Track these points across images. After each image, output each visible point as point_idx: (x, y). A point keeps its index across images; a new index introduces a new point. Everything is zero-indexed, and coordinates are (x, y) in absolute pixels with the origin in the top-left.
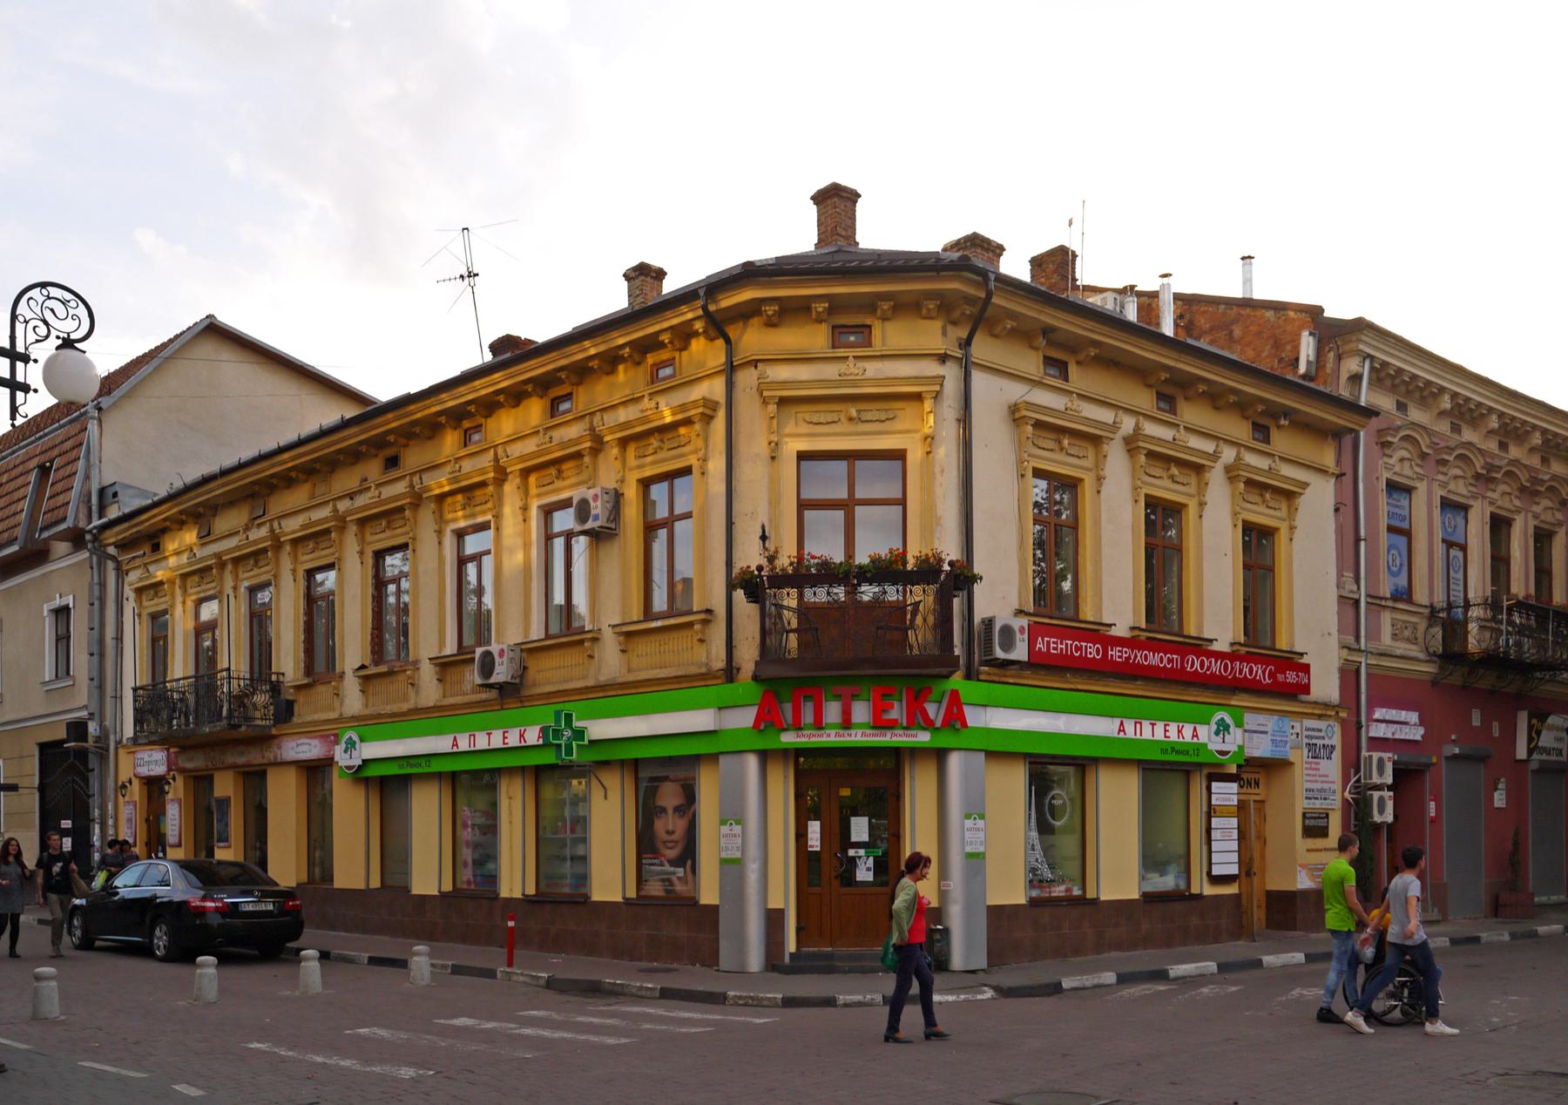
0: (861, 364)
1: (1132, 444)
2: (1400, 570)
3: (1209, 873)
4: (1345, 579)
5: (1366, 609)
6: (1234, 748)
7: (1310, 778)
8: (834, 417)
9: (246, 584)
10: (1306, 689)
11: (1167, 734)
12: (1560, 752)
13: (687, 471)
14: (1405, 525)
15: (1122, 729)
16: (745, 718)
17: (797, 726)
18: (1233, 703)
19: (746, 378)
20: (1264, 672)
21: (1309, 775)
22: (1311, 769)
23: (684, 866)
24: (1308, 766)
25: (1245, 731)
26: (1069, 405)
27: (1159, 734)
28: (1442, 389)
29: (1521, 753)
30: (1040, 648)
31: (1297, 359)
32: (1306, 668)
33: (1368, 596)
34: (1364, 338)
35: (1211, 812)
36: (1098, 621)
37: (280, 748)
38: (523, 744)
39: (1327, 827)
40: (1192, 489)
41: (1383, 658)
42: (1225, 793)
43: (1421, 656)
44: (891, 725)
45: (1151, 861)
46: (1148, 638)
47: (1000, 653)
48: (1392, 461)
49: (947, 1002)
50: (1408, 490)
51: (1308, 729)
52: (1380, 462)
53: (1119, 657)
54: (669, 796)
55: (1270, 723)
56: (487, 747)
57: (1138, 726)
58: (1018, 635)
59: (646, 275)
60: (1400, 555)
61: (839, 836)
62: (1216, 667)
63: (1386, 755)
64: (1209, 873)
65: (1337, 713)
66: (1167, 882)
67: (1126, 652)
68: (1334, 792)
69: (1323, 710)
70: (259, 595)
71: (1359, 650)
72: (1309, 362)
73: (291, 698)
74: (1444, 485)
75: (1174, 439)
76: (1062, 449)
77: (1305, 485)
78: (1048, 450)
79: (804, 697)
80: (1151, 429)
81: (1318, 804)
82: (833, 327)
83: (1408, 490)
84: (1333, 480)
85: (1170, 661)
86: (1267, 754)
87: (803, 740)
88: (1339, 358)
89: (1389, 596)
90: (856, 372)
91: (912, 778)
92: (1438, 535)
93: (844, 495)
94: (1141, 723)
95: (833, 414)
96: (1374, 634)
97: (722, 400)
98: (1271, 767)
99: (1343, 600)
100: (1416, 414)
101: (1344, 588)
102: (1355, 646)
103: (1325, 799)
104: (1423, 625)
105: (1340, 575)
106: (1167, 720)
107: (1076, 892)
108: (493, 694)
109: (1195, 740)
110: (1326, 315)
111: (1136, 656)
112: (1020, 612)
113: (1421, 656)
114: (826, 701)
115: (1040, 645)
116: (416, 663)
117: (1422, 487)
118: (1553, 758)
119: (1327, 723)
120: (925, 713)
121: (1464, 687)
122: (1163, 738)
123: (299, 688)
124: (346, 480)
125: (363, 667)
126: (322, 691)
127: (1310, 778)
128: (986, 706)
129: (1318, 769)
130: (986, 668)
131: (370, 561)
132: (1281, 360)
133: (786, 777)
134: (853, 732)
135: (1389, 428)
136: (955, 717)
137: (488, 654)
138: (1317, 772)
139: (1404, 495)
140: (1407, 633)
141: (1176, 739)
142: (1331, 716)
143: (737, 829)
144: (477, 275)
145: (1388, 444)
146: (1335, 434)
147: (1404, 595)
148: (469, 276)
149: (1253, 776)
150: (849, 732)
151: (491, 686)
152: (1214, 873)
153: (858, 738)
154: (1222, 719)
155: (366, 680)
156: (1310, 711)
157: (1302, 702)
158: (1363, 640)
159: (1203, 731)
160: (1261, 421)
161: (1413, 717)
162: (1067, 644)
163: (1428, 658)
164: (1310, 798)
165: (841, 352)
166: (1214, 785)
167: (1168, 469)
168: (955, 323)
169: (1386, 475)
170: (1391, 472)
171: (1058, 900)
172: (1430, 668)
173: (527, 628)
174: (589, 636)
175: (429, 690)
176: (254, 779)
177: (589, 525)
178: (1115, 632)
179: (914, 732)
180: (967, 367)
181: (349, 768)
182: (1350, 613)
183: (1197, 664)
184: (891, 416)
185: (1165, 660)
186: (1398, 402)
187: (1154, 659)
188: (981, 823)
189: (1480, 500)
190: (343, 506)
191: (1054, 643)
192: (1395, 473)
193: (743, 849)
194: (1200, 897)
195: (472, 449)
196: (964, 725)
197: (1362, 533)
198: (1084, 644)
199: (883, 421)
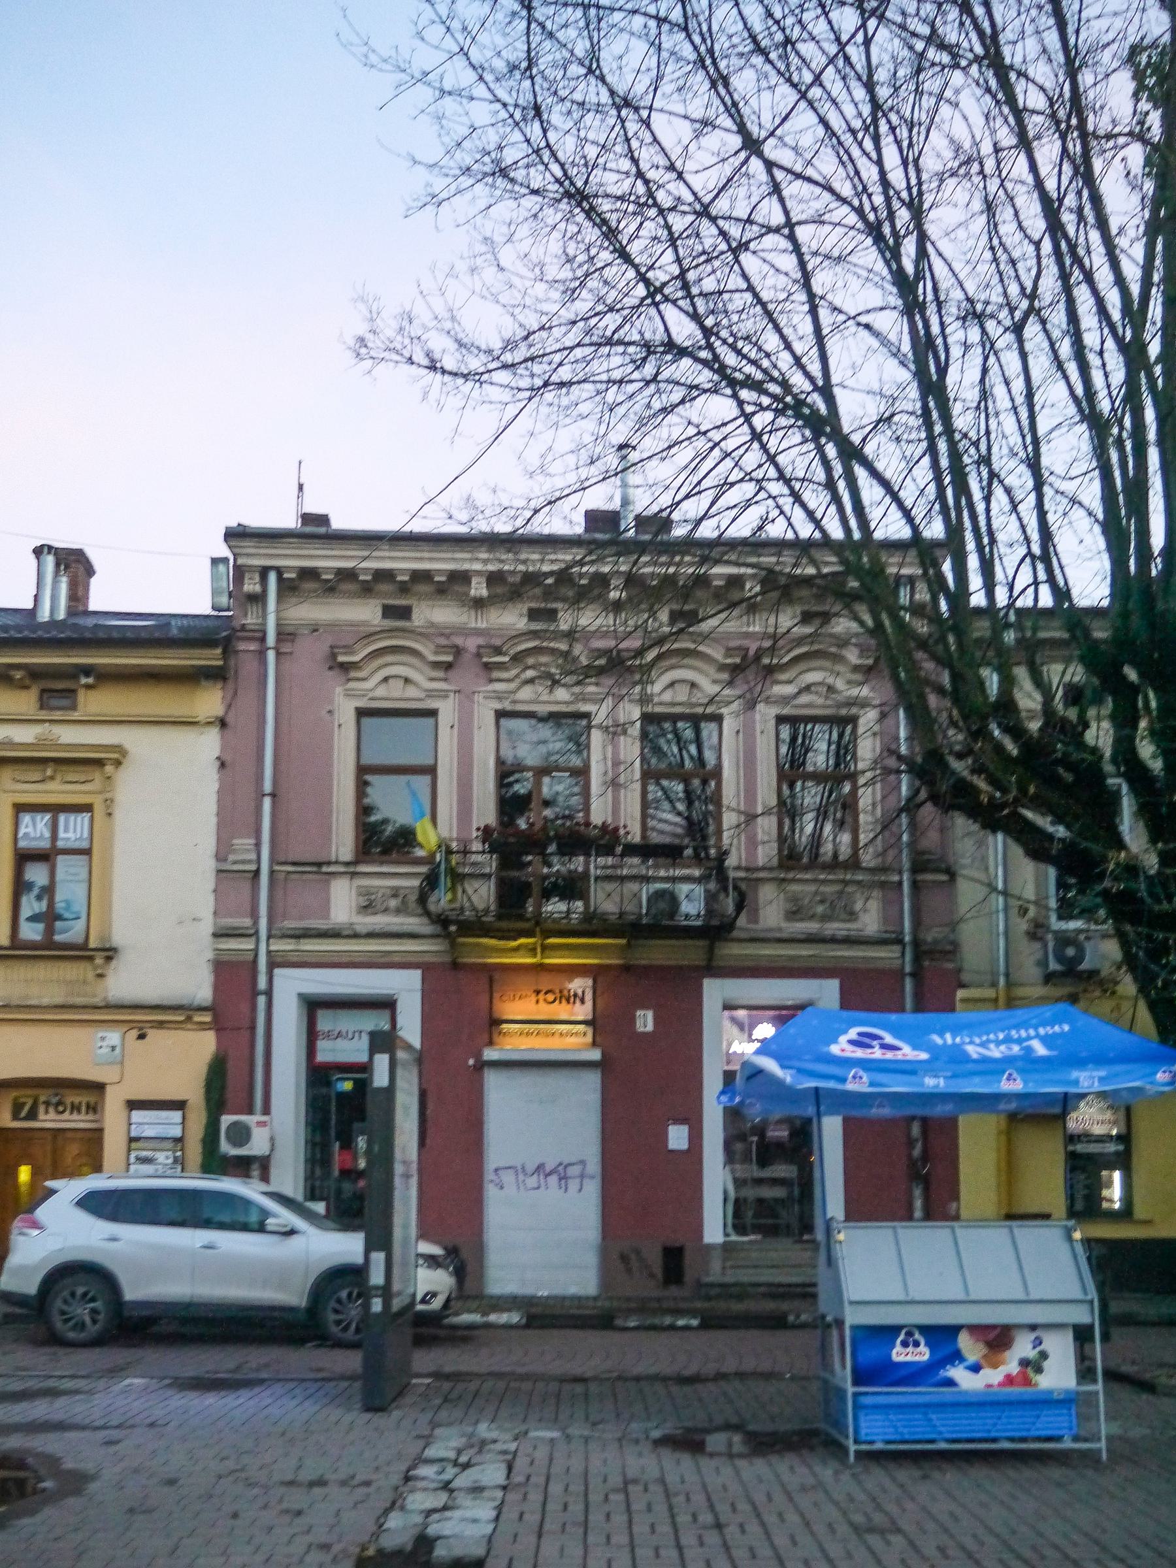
50: (433, 713)
96: (325, 908)
117: (447, 710)
146: (217, 675)
192: (372, 699)
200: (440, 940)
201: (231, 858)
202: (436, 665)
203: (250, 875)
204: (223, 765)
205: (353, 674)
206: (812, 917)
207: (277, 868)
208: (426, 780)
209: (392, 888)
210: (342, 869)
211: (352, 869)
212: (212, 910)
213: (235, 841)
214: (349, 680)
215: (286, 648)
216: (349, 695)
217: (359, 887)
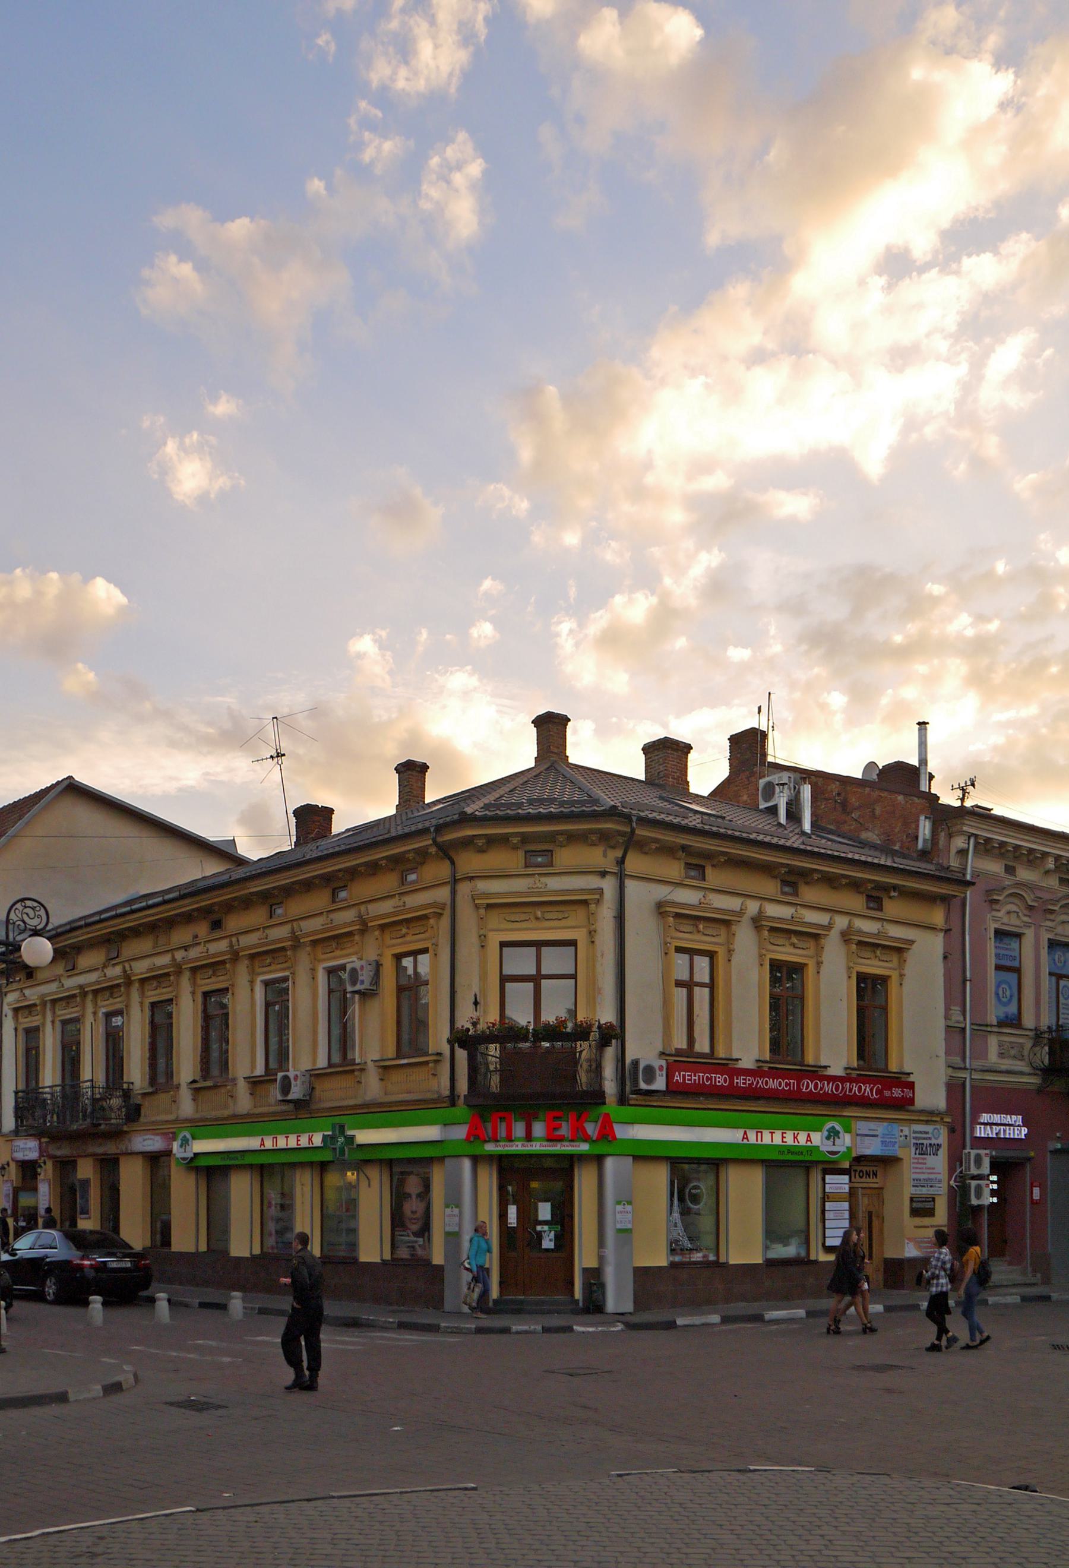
0: (544, 880)
1: (758, 922)
2: (1010, 1000)
3: (824, 1244)
4: (952, 1012)
5: (971, 1035)
6: (843, 1149)
7: (918, 1171)
8: (524, 917)
9: (104, 1010)
10: (911, 1101)
11: (784, 1140)
13: (425, 951)
14: (1016, 964)
15: (745, 1137)
16: (460, 1132)
17: (495, 1139)
18: (845, 1114)
19: (464, 888)
20: (871, 1090)
21: (917, 1168)
22: (918, 1163)
23: (423, 1237)
24: (916, 1161)
25: (857, 1135)
26: (703, 900)
27: (777, 1139)
28: (1045, 855)
30: (677, 1080)
31: (917, 838)
32: (911, 1086)
33: (972, 1024)
34: (966, 822)
35: (825, 1198)
36: (728, 1057)
37: (130, 1141)
38: (311, 1145)
39: (933, 1209)
40: (811, 952)
41: (988, 1073)
42: (838, 1183)
43: (1027, 1069)
44: (560, 1139)
45: (773, 1234)
46: (770, 1068)
47: (643, 1086)
48: (999, 914)
49: (589, 1332)
50: (1019, 936)
51: (915, 1132)
52: (989, 915)
53: (743, 1084)
54: (413, 1185)
55: (880, 1128)
56: (286, 1147)
57: (759, 1134)
58: (658, 1072)
59: (413, 770)
60: (1010, 988)
61: (527, 1216)
62: (829, 1088)
63: (982, 1152)
64: (824, 1244)
65: (942, 1119)
66: (790, 1250)
67: (749, 1080)
68: (940, 1181)
69: (930, 1116)
70: (113, 1019)
71: (965, 1069)
72: (925, 840)
73: (139, 1102)
74: (1050, 930)
75: (792, 917)
76: (699, 932)
77: (911, 942)
78: (687, 933)
79: (501, 1118)
80: (773, 910)
81: (924, 1191)
82: (526, 852)
83: (1019, 936)
84: (942, 934)
85: (787, 1084)
86: (878, 1153)
87: (500, 1148)
88: (950, 836)
89: (995, 1023)
90: (540, 886)
91: (580, 1176)
92: (1045, 970)
93: (533, 972)
94: (761, 1132)
95: (524, 915)
96: (984, 1054)
97: (449, 903)
98: (887, 1162)
99: (949, 1029)
100: (1025, 874)
101: (950, 1020)
102: (962, 1066)
103: (931, 1186)
104: (1029, 1044)
105: (947, 1009)
106: (784, 1128)
107: (712, 1258)
108: (291, 1106)
109: (809, 1143)
110: (940, 802)
111: (758, 1082)
112: (662, 1054)
113: (1027, 1069)
114: (515, 1121)
115: (677, 1078)
116: (234, 1080)
117: (1029, 934)
119: (935, 1127)
120: (584, 1130)
122: (781, 1143)
123: (144, 1095)
124: (181, 936)
125: (194, 1081)
126: (163, 1098)
127: (918, 1171)
128: (633, 1123)
129: (925, 1164)
130: (634, 1096)
131: (200, 999)
132: (908, 836)
133: (491, 1174)
134: (534, 1143)
135: (994, 890)
136: (607, 1133)
137: (286, 1078)
138: (924, 1166)
139: (1014, 939)
140: (1013, 1052)
141: (792, 1144)
142: (936, 1121)
143: (456, 1211)
144: (284, 755)
145: (997, 901)
146: (945, 899)
147: (1014, 1022)
148: (278, 756)
149: (871, 1169)
150: (532, 1143)
151: (289, 1101)
152: (827, 1244)
153: (537, 1147)
154: (833, 1127)
155: (197, 1092)
156: (916, 1118)
157: (907, 1111)
158: (968, 1060)
159: (817, 1138)
160: (874, 894)
161: (1018, 1119)
162: (699, 1076)
163: (1032, 1072)
164: (917, 1186)
165: (530, 871)
166: (828, 1177)
167: (790, 938)
168: (613, 847)
169: (993, 926)
171: (695, 1263)
172: (1035, 1080)
173: (314, 1061)
174: (358, 1067)
175: (244, 1102)
176: (109, 1165)
177: (358, 987)
178: (742, 1065)
179: (578, 1143)
180: (621, 878)
181: (184, 1159)
182: (957, 1037)
183: (812, 1086)
184: (566, 916)
185: (783, 1084)
186: (1006, 865)
187: (773, 1084)
188: (629, 1208)
190: (179, 955)
191: (688, 1075)
192: (1002, 924)
193: (460, 1225)
194: (816, 1262)
195: (273, 921)
196: (615, 1138)
198: (713, 1075)
199: (560, 920)
201: (954, 1018)
208: (1015, 975)
209: (1011, 1042)
212: (944, 1051)
213: (952, 1008)
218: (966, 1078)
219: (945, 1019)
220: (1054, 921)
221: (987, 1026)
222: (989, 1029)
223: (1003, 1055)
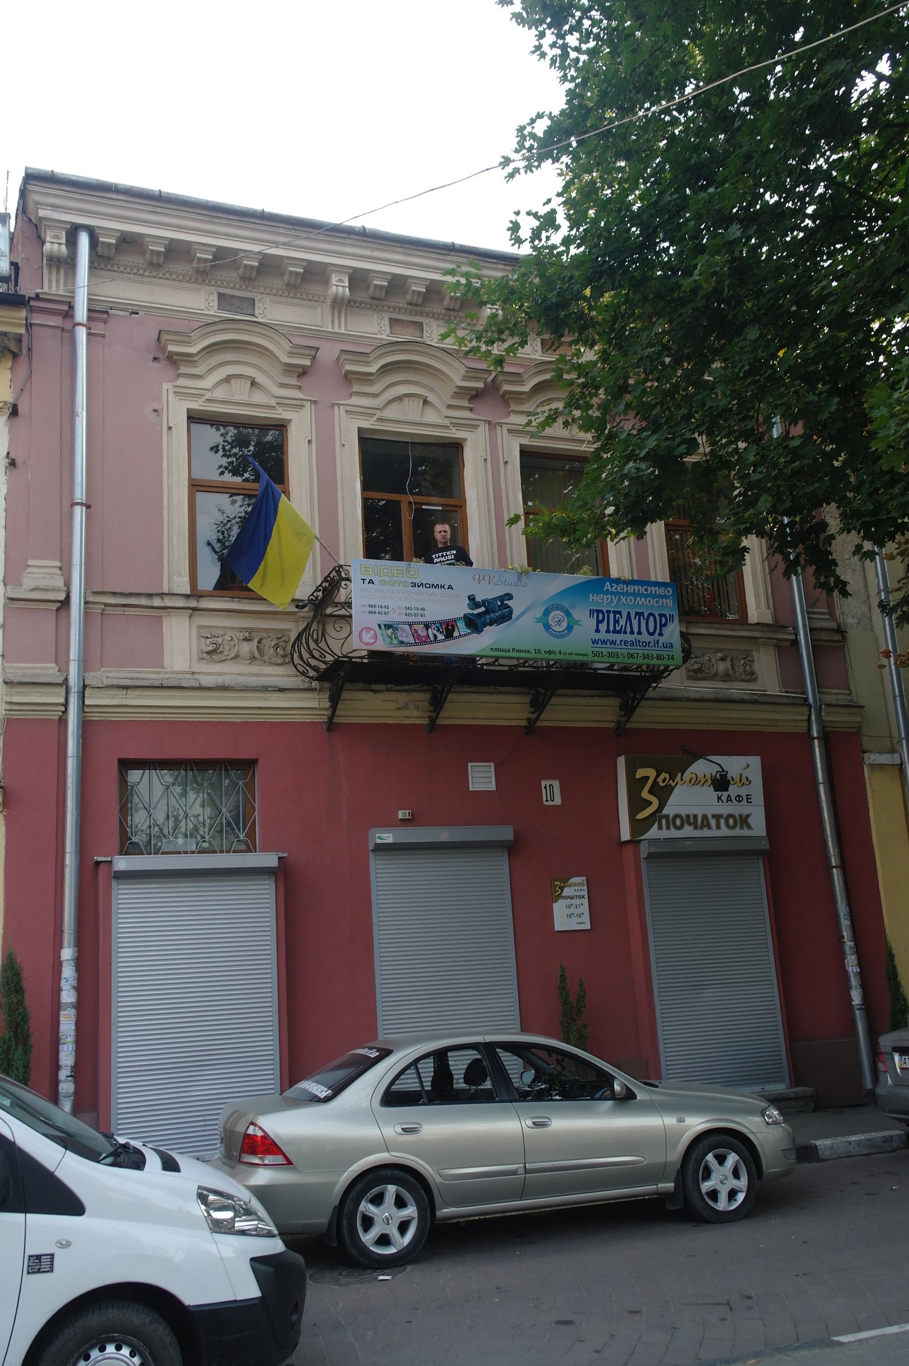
4: (30, 570)
12: (744, 821)
29: (626, 834)
48: (207, 383)
96: (156, 657)
118: (724, 831)
121: (433, 726)
163: (306, 685)
170: (206, 397)
189: (483, 430)
192: (208, 400)
197: (80, 493)
200: (314, 695)
201: (28, 583)
202: (289, 369)
203: (54, 607)
204: (13, 463)
205: (183, 370)
206: (714, 677)
207: (91, 598)
209: (241, 630)
210: (181, 603)
211: (193, 603)
213: (30, 562)
214: (179, 376)
215: (98, 328)
216: (180, 394)
217: (199, 627)
218: (66, 704)
219: (5, 585)
220: (375, 396)
221: (150, 596)
222: (157, 602)
223: (215, 657)
